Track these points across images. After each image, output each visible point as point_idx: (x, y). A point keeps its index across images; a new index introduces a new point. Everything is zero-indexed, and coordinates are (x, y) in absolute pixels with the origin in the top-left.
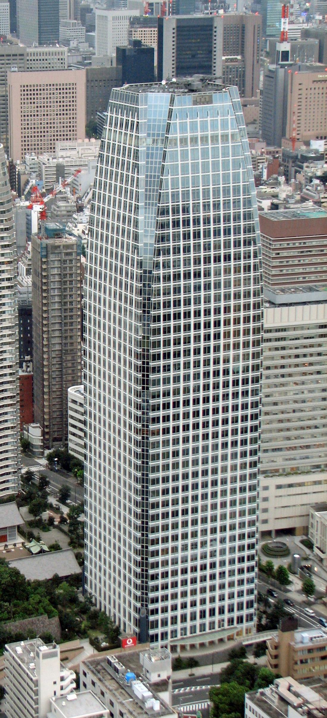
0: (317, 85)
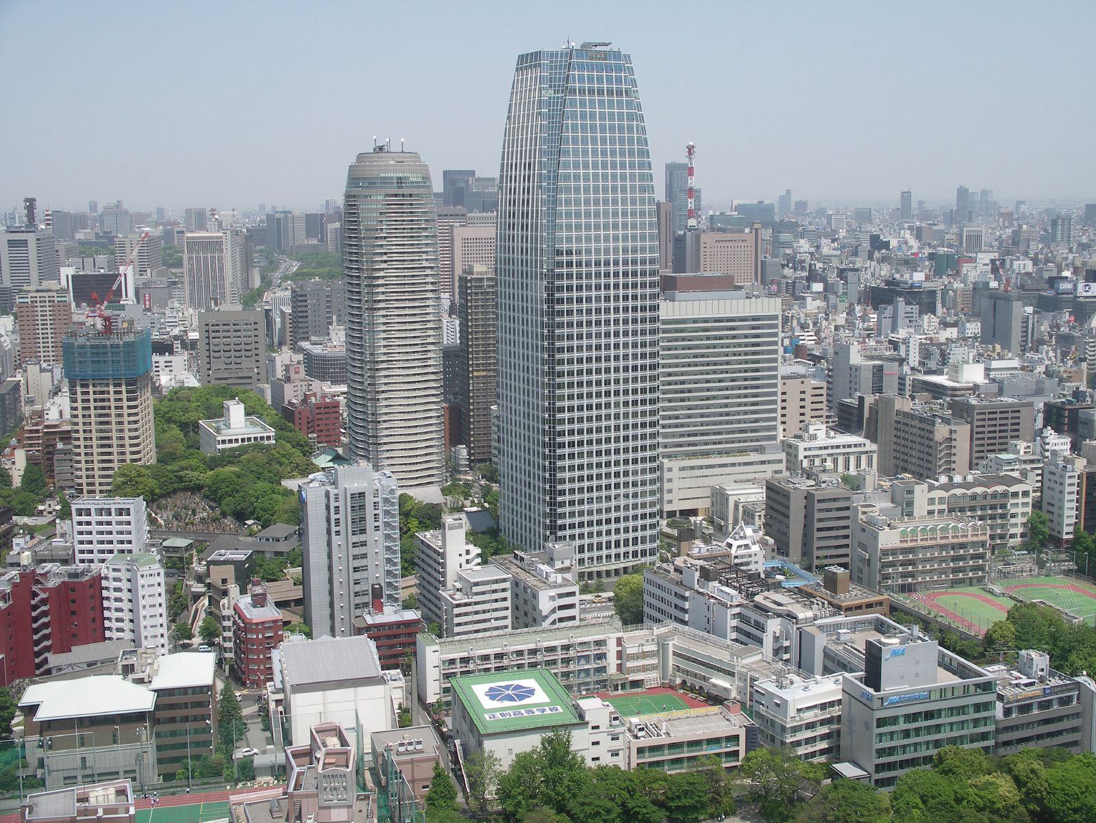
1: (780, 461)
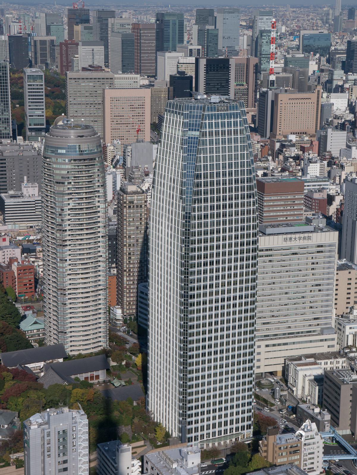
0: (291, 101)
1: (333, 339)
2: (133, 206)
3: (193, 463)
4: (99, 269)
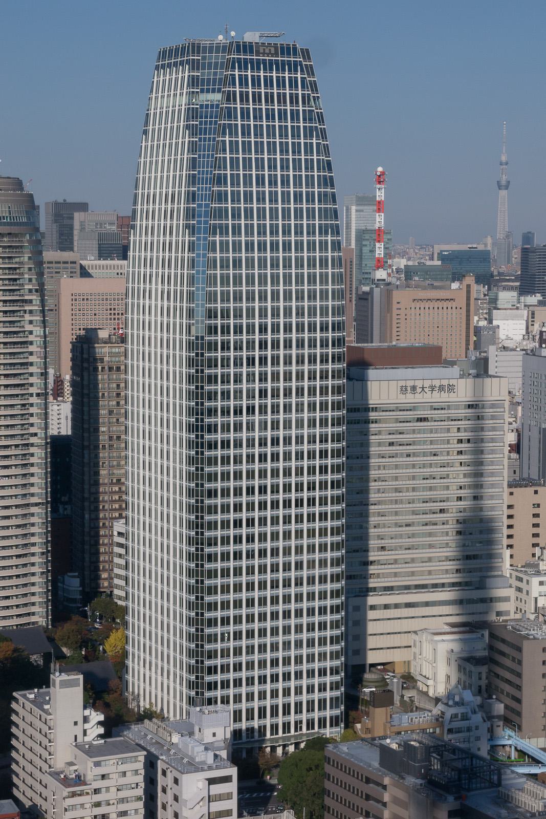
0: (418, 305)
2: (103, 368)
3: (214, 735)
4: (32, 460)
